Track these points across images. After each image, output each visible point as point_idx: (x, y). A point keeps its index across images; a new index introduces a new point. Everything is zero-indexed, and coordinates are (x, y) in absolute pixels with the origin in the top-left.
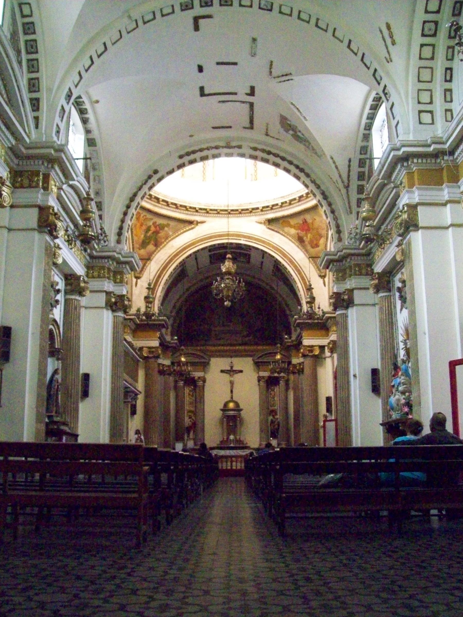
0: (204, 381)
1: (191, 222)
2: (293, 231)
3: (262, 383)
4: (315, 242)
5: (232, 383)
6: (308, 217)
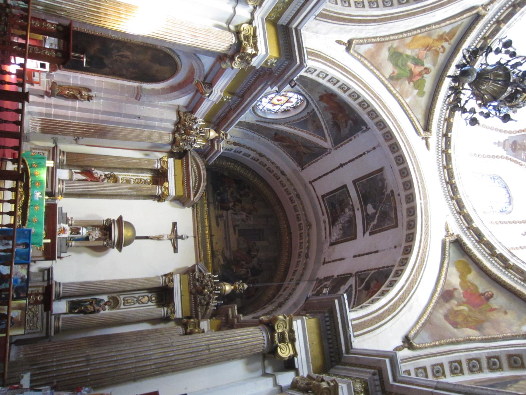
0: (160, 198)
1: (427, 128)
2: (455, 280)
3: (161, 282)
4: (459, 319)
5: (158, 238)
6: (499, 300)
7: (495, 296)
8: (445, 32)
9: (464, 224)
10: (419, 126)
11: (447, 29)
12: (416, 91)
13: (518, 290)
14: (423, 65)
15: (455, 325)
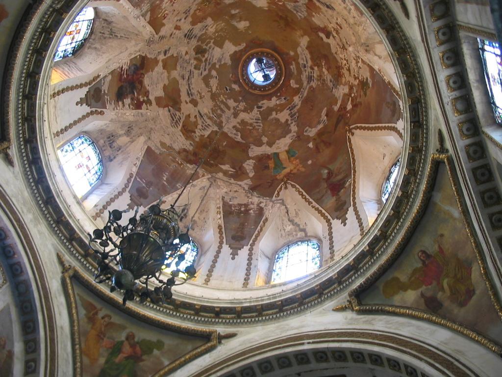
1: (206, 337)
2: (411, 296)
4: (463, 288)
6: (426, 243)
7: (423, 249)
8: (85, 315)
9: (335, 288)
10: (203, 348)
11: (83, 312)
12: (156, 352)
13: (411, 224)
14: (122, 342)
15: (470, 293)
